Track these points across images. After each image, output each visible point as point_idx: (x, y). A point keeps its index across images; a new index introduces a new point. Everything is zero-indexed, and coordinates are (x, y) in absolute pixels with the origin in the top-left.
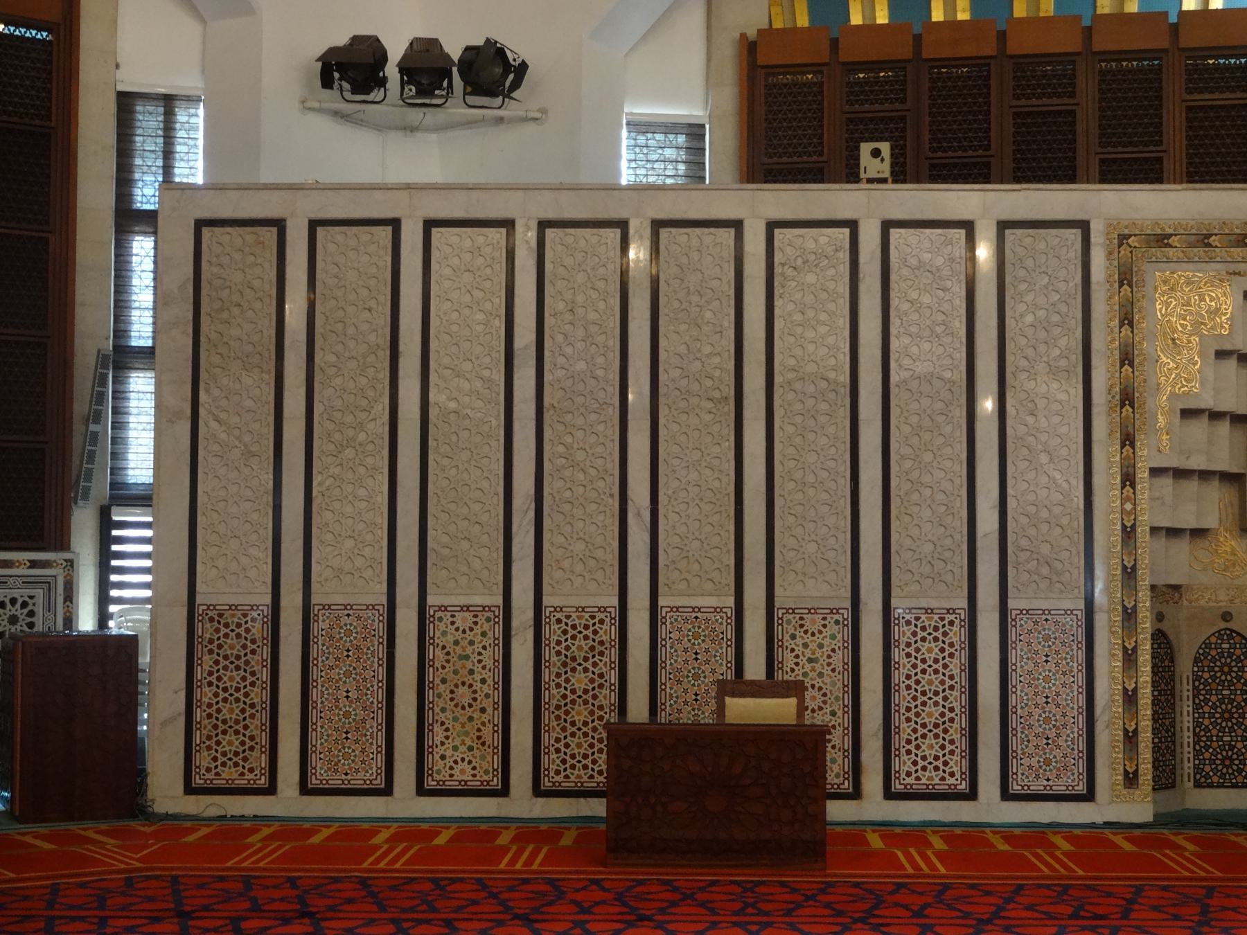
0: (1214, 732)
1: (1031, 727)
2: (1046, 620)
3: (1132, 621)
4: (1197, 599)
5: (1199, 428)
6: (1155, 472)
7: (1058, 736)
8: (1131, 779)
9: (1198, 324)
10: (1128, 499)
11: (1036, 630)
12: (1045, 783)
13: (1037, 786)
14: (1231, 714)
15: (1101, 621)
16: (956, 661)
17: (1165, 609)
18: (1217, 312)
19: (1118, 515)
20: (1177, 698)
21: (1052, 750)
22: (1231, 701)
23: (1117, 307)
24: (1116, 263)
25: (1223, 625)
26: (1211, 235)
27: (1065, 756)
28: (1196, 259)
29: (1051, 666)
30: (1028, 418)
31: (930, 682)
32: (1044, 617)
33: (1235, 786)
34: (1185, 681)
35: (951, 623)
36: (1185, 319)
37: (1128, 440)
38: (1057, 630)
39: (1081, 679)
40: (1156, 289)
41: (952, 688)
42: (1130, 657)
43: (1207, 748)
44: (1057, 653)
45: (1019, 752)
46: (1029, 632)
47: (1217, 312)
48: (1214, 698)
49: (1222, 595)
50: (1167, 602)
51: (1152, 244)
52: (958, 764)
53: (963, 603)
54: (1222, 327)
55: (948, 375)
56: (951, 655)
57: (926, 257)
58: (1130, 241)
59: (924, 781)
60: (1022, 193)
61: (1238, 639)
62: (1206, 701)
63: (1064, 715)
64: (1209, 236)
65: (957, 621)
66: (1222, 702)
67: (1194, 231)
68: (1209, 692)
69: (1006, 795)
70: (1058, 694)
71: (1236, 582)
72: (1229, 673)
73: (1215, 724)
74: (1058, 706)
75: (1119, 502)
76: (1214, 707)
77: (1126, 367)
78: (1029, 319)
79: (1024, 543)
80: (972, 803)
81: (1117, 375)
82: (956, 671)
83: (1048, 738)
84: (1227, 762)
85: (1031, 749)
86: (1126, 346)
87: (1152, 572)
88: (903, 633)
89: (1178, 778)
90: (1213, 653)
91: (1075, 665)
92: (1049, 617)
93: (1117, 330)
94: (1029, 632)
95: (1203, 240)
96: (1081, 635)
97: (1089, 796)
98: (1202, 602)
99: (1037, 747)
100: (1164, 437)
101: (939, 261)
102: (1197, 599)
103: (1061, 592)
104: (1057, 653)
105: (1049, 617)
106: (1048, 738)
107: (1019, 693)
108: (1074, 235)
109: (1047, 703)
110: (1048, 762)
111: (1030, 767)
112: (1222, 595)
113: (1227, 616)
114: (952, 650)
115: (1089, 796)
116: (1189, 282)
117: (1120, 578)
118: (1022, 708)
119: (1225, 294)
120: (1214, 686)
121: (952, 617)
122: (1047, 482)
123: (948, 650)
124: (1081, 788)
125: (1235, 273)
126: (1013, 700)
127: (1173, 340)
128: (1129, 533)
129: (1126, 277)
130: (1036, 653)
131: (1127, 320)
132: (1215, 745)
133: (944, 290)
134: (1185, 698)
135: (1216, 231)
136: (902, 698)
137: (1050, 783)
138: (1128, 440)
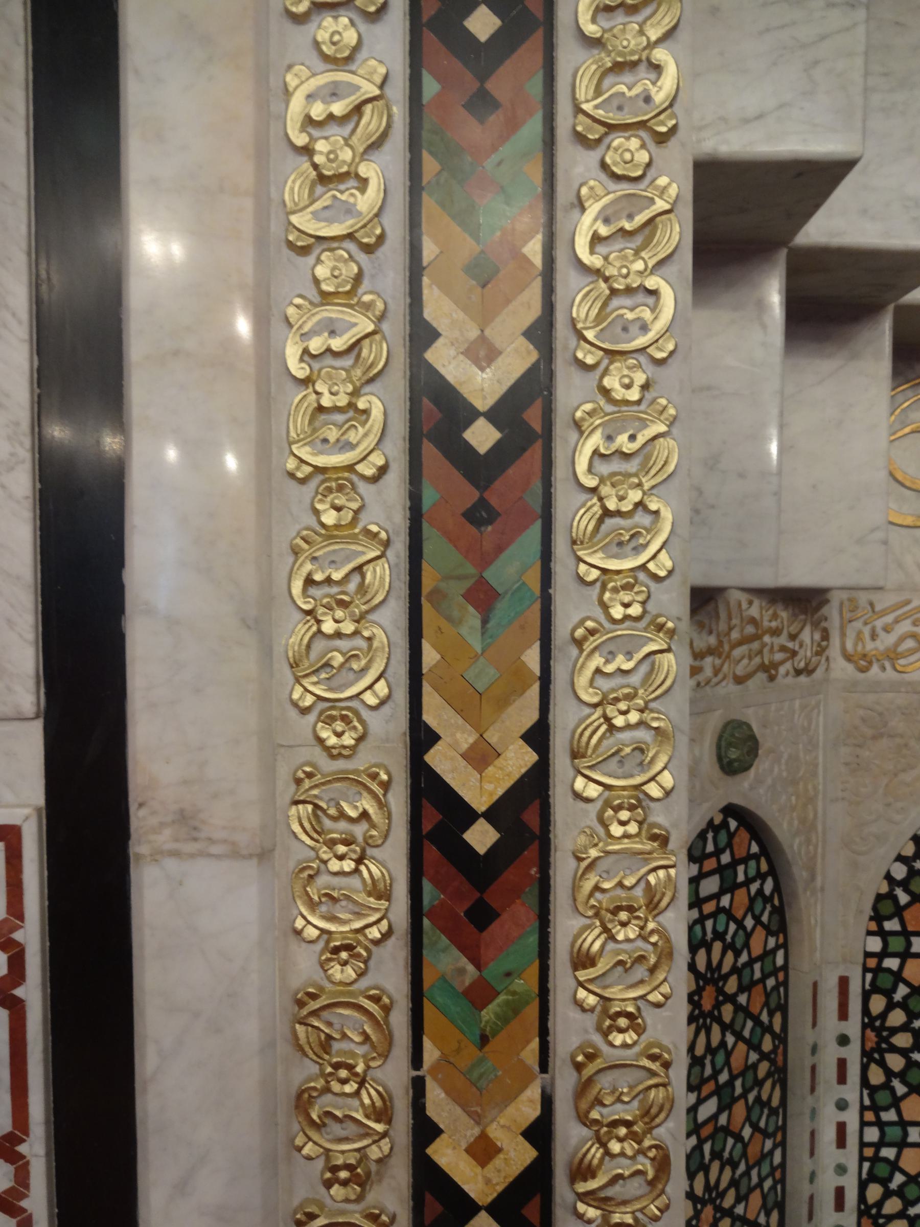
3: (513, 953)
17: (756, 705)
20: (798, 1080)
87: (698, 514)
102: (892, 655)
117: (386, 509)
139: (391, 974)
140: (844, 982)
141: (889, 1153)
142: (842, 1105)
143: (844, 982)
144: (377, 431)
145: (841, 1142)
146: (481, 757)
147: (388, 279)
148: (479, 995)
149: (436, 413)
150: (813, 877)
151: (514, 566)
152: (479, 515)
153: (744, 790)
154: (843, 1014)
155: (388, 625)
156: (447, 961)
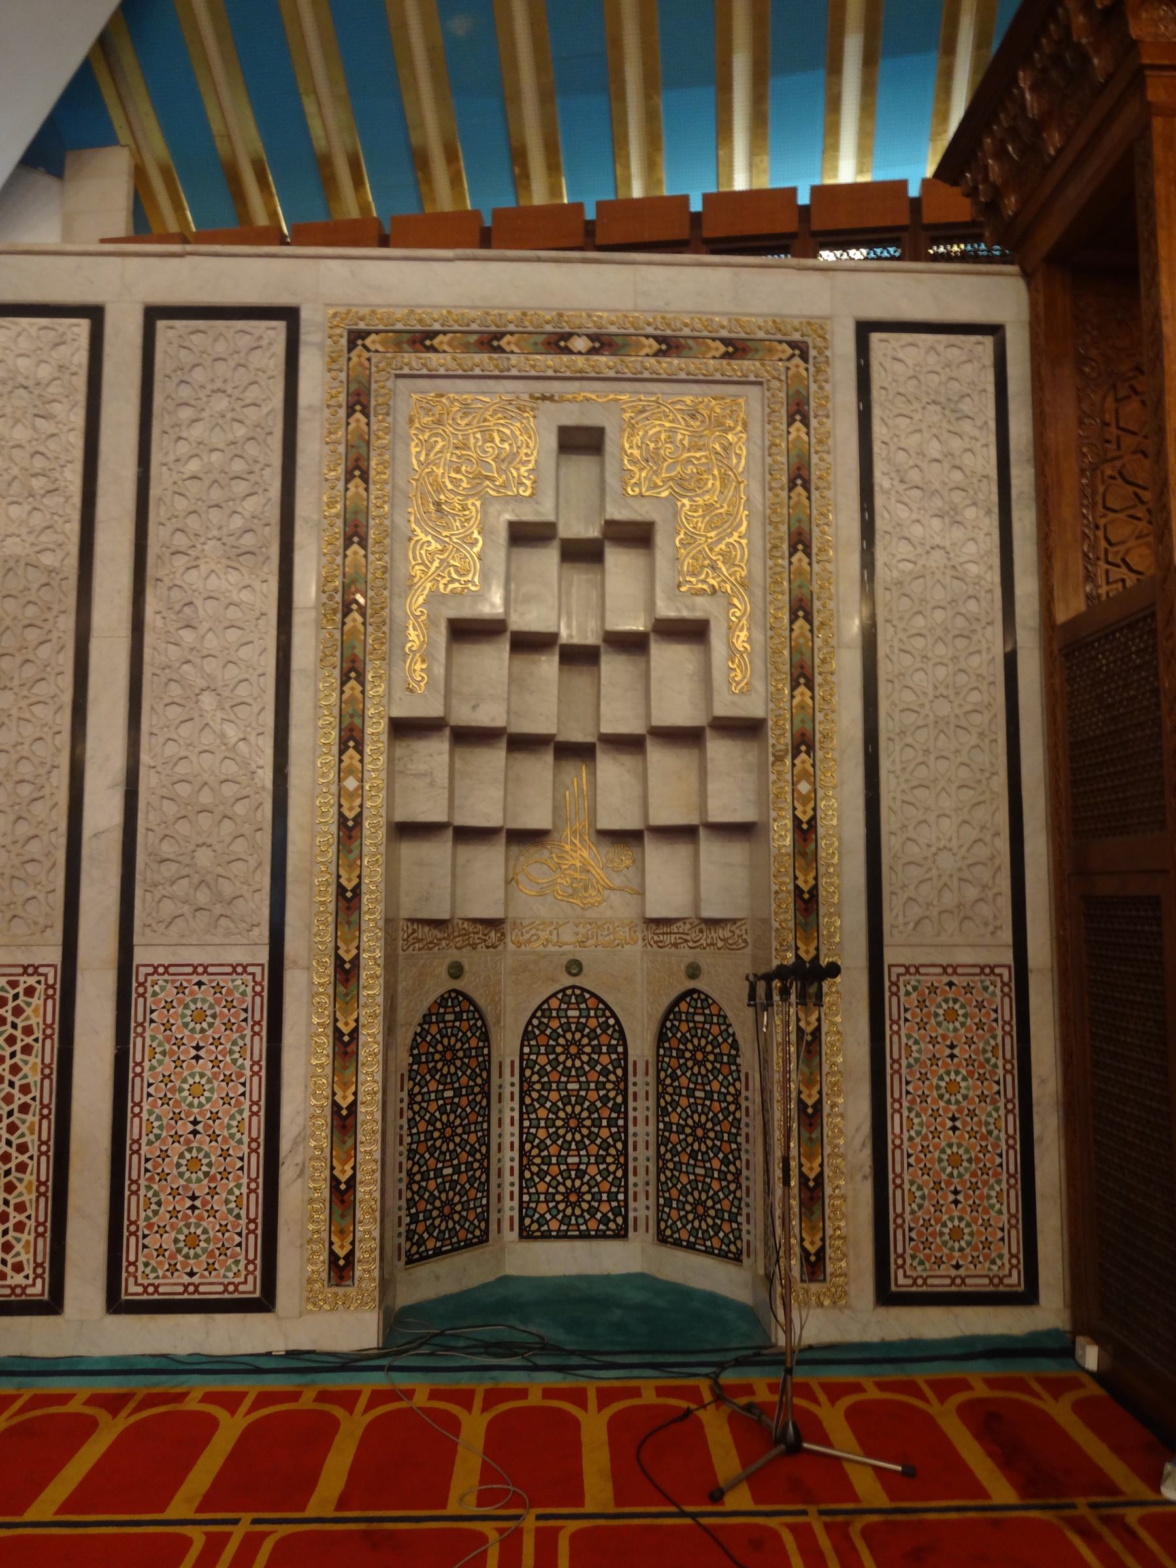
0: (554, 1150)
1: (164, 1176)
2: (200, 984)
3: (353, 987)
4: (529, 941)
5: (491, 661)
6: (404, 729)
7: (213, 1192)
8: (341, 1269)
9: (479, 478)
10: (351, 771)
11: (180, 1001)
12: (186, 1279)
13: (172, 1287)
14: (580, 1121)
15: (295, 983)
16: (34, 1059)
18: (506, 460)
19: (333, 800)
21: (200, 1218)
22: (581, 1101)
23: (342, 449)
24: (343, 376)
25: (569, 981)
26: (503, 334)
27: (224, 1229)
28: (477, 371)
29: (205, 1065)
30: (182, 632)
32: (195, 979)
33: (584, 1236)
34: (507, 1070)
35: (30, 991)
36: (458, 471)
37: (352, 670)
38: (218, 1002)
39: (258, 1088)
40: (411, 421)
41: (24, 1108)
42: (345, 1047)
43: (542, 1174)
45: (142, 1224)
46: (169, 1005)
47: (506, 460)
48: (554, 1096)
49: (567, 935)
50: (474, 946)
51: (406, 347)
52: (29, 1249)
53: (54, 955)
54: (522, 484)
55: (48, 559)
56: (27, 1050)
58: (368, 342)
60: (189, 259)
61: (592, 1003)
62: (542, 1100)
63: (225, 1154)
64: (499, 336)
65: (40, 988)
66: (566, 1101)
67: (474, 327)
68: (546, 1087)
69: (116, 1303)
70: (215, 1117)
71: (590, 914)
72: (578, 1056)
73: (554, 1137)
74: (214, 1137)
75: (332, 775)
76: (554, 1109)
77: (355, 547)
78: (193, 466)
79: (167, 849)
80: (51, 1319)
81: (339, 560)
82: (34, 1078)
83: (193, 1198)
84: (573, 1198)
85: (163, 1218)
86: (356, 513)
89: (493, 1227)
90: (555, 1024)
91: (248, 1063)
92: (204, 978)
93: (341, 485)
94: (169, 1005)
95: (490, 342)
96: (261, 1012)
97: (265, 1303)
98: (537, 946)
99: (174, 1213)
100: (418, 666)
101: (45, 372)
102: (529, 941)
103: (228, 933)
104: (217, 1042)
105: (204, 978)
106: (193, 1198)
107: (145, 1115)
108: (276, 330)
109: (195, 1133)
111: (161, 1251)
112: (567, 935)
113: (574, 967)
114: (29, 1040)
115: (265, 1303)
116: (466, 410)
117: (332, 907)
118: (150, 1143)
119: (526, 430)
120: (554, 1076)
121: (31, 981)
122: (210, 743)
123: (22, 1040)
124: (251, 1288)
125: (544, 398)
126: (134, 1129)
127: (438, 504)
128: (349, 830)
129: (359, 401)
130: (179, 1043)
131: (357, 469)
132: (554, 1170)
134: (507, 1096)
135: (511, 328)
137: (196, 1279)
138: (352, 670)
139: (331, 991)
140: (512, 1063)
141: (533, 1131)
142: (512, 1110)
143: (512, 1063)
144: (330, 897)
145: (512, 1124)
146: (348, 951)
147: (333, 868)
148: (346, 995)
149: (341, 889)
150: (499, 1021)
151: (354, 918)
152: (348, 908)
153: (459, 985)
154: (512, 1075)
155: (331, 928)
156: (341, 989)
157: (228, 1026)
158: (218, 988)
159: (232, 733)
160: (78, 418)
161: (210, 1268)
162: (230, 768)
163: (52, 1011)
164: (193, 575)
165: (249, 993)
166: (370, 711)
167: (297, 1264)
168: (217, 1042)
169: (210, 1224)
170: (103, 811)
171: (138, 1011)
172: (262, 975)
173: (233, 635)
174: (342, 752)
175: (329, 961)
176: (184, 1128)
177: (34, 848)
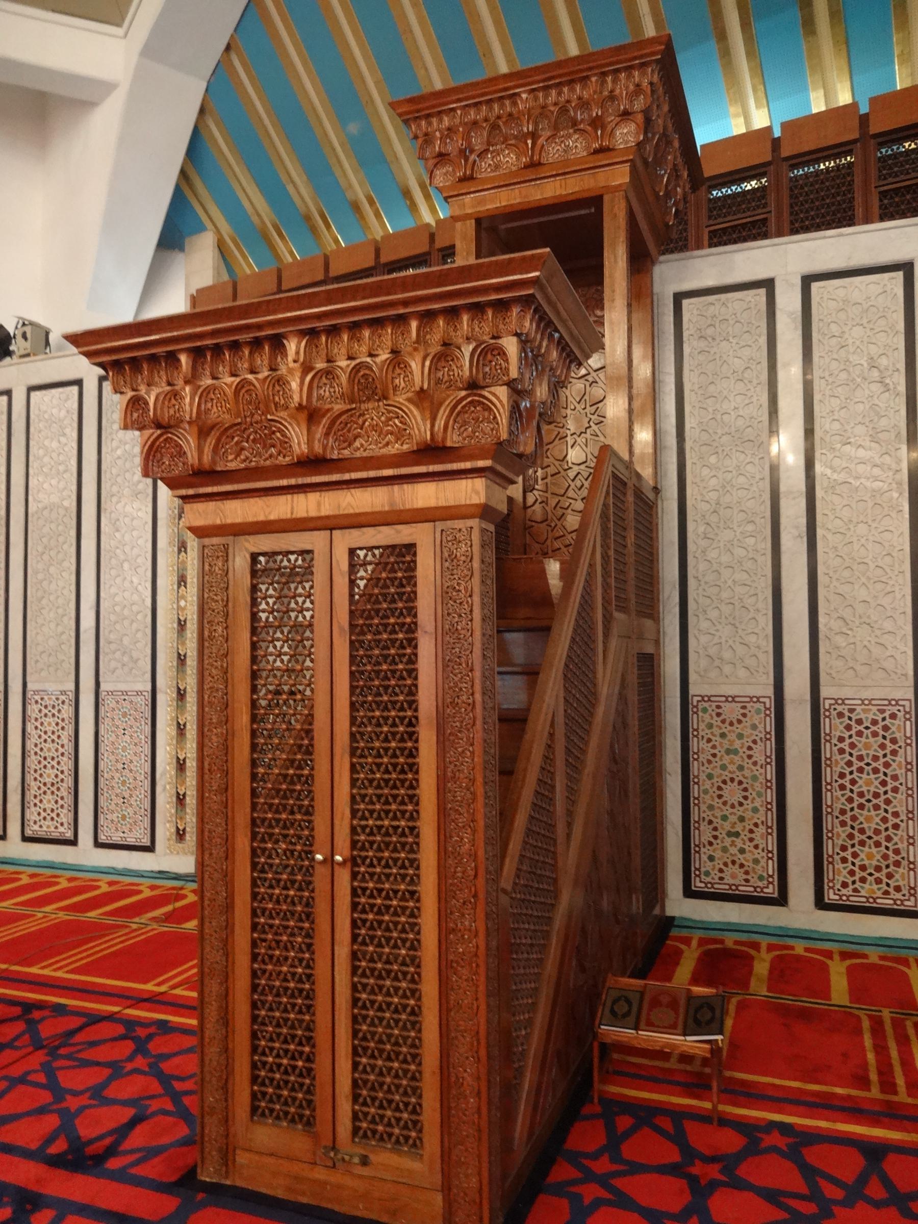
7: (131, 796)
8: (180, 835)
10: (183, 597)
13: (116, 838)
15: (160, 698)
27: (135, 813)
29: (127, 738)
31: (50, 750)
39: (147, 749)
44: (131, 727)
52: (66, 816)
53: (72, 686)
57: (55, 411)
59: (45, 828)
63: (135, 779)
70: (131, 762)
74: (131, 771)
79: (112, 637)
88: (33, 710)
96: (148, 714)
99: (117, 805)
110: (124, 818)
111: (112, 821)
115: (150, 849)
130: (117, 727)
133: (64, 435)
136: (32, 762)
157: (135, 719)
158: (131, 702)
159: (135, 580)
160: (75, 435)
161: (131, 830)
162: (135, 597)
163: (71, 710)
164: (119, 506)
165: (143, 703)
166: (189, 567)
167: (164, 831)
168: (131, 727)
169: (130, 810)
170: (87, 621)
171: (102, 713)
172: (149, 696)
173: (135, 533)
174: (179, 587)
175: (175, 690)
176: (120, 766)
177: (64, 637)
